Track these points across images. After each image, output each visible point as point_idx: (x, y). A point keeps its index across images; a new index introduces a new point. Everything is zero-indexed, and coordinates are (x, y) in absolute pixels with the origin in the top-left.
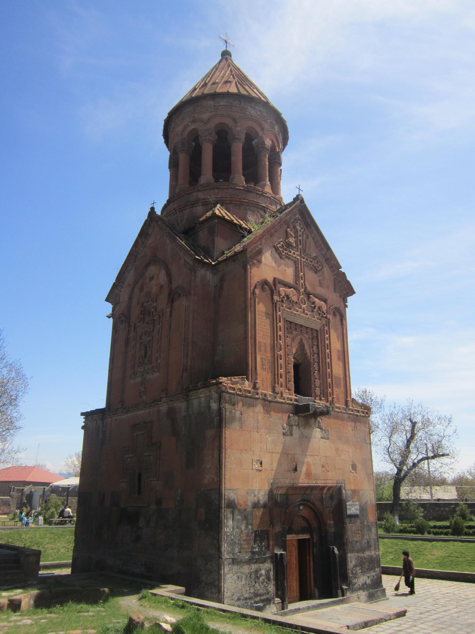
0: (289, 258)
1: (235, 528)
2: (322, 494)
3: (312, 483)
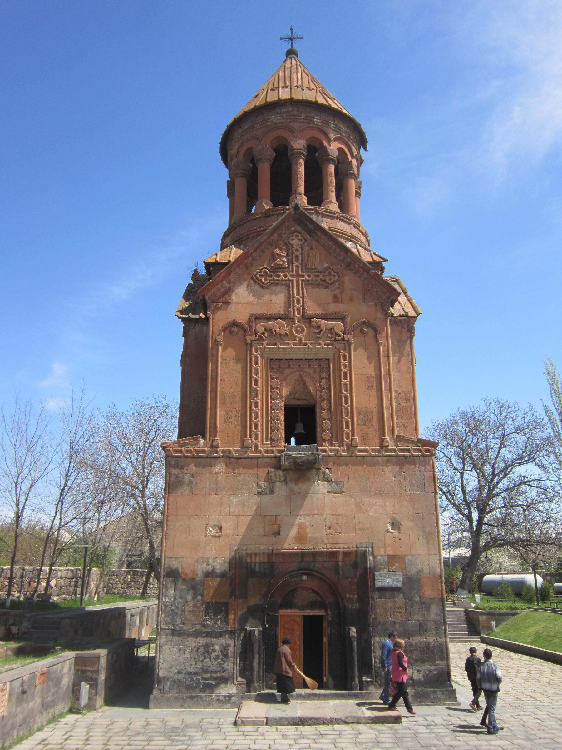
0: (277, 284)
1: (177, 598)
2: (338, 562)
3: (309, 548)
